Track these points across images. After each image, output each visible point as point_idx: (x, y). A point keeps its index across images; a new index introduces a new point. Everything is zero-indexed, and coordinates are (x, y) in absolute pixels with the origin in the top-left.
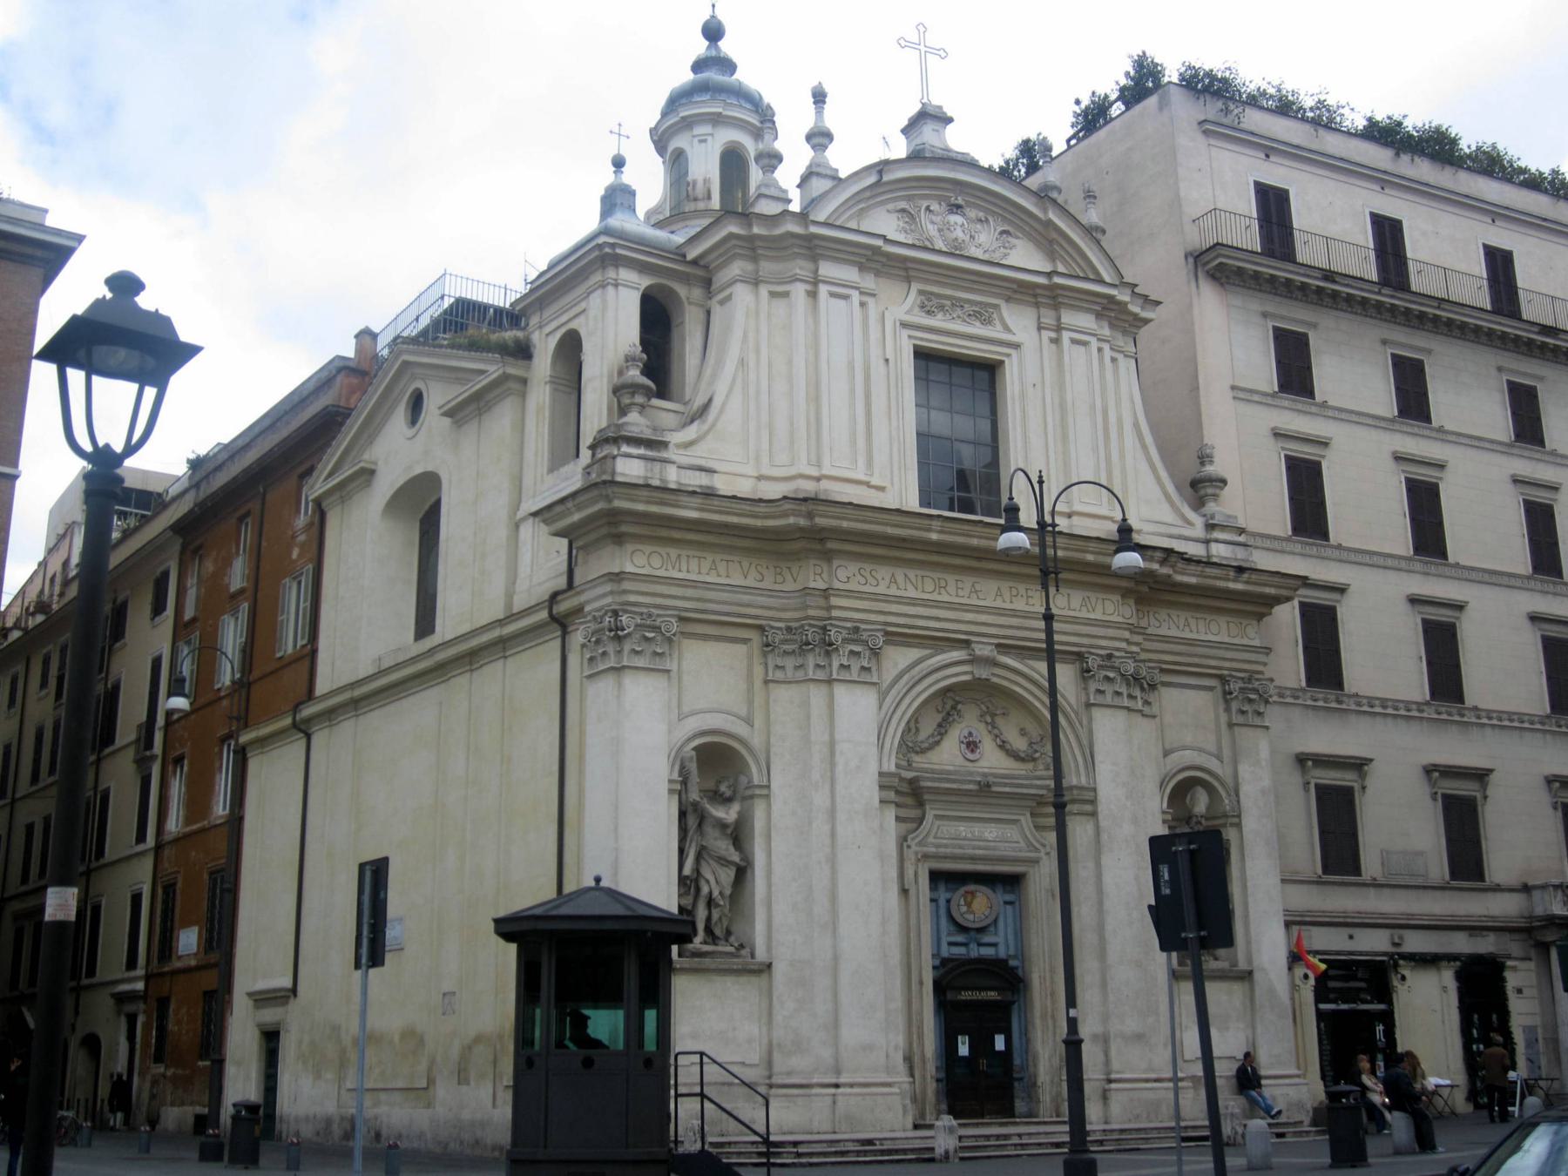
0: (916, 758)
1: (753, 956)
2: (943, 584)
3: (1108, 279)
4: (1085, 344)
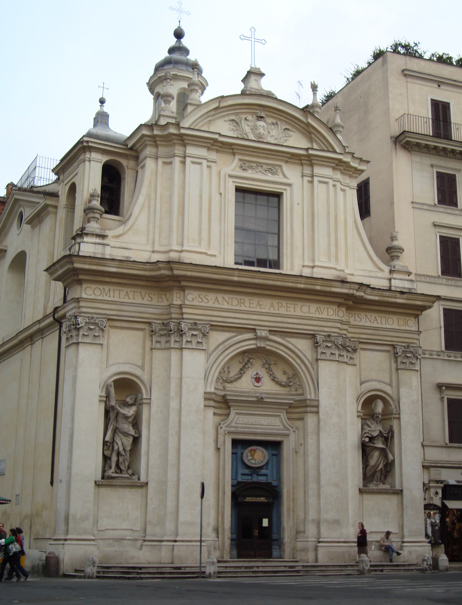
0: (227, 385)
1: (139, 479)
2: (242, 301)
3: (338, 151)
4: (326, 183)
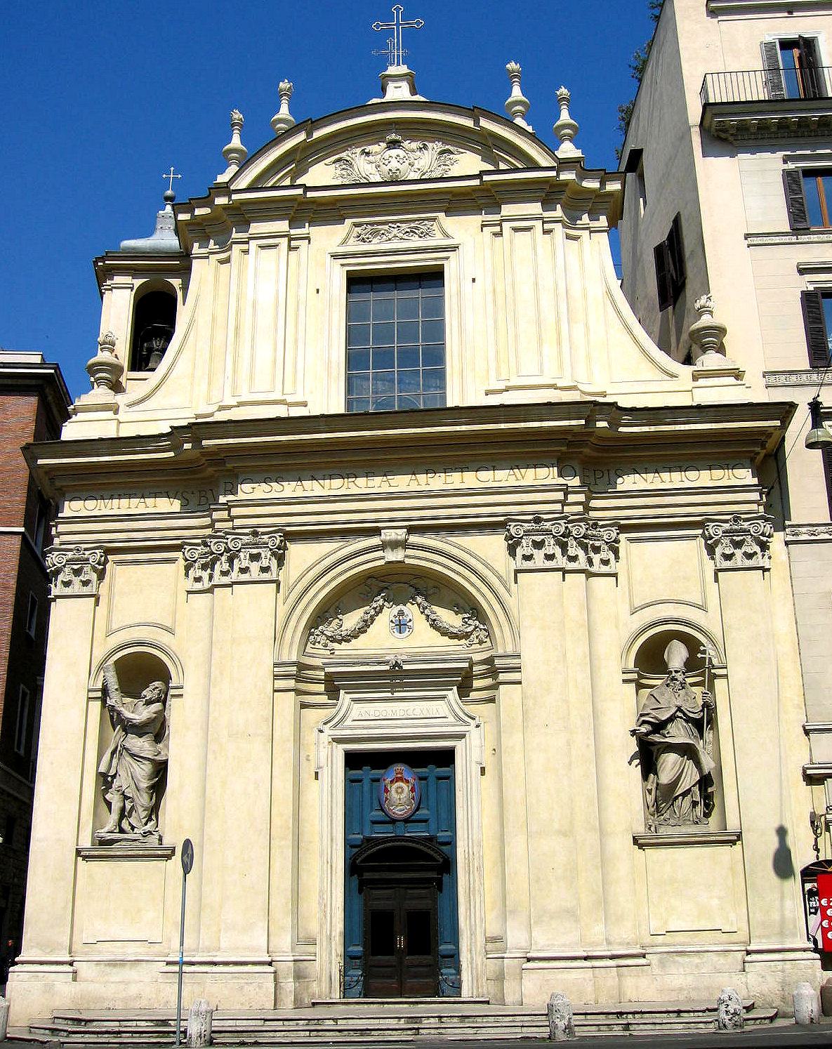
0: (336, 645)
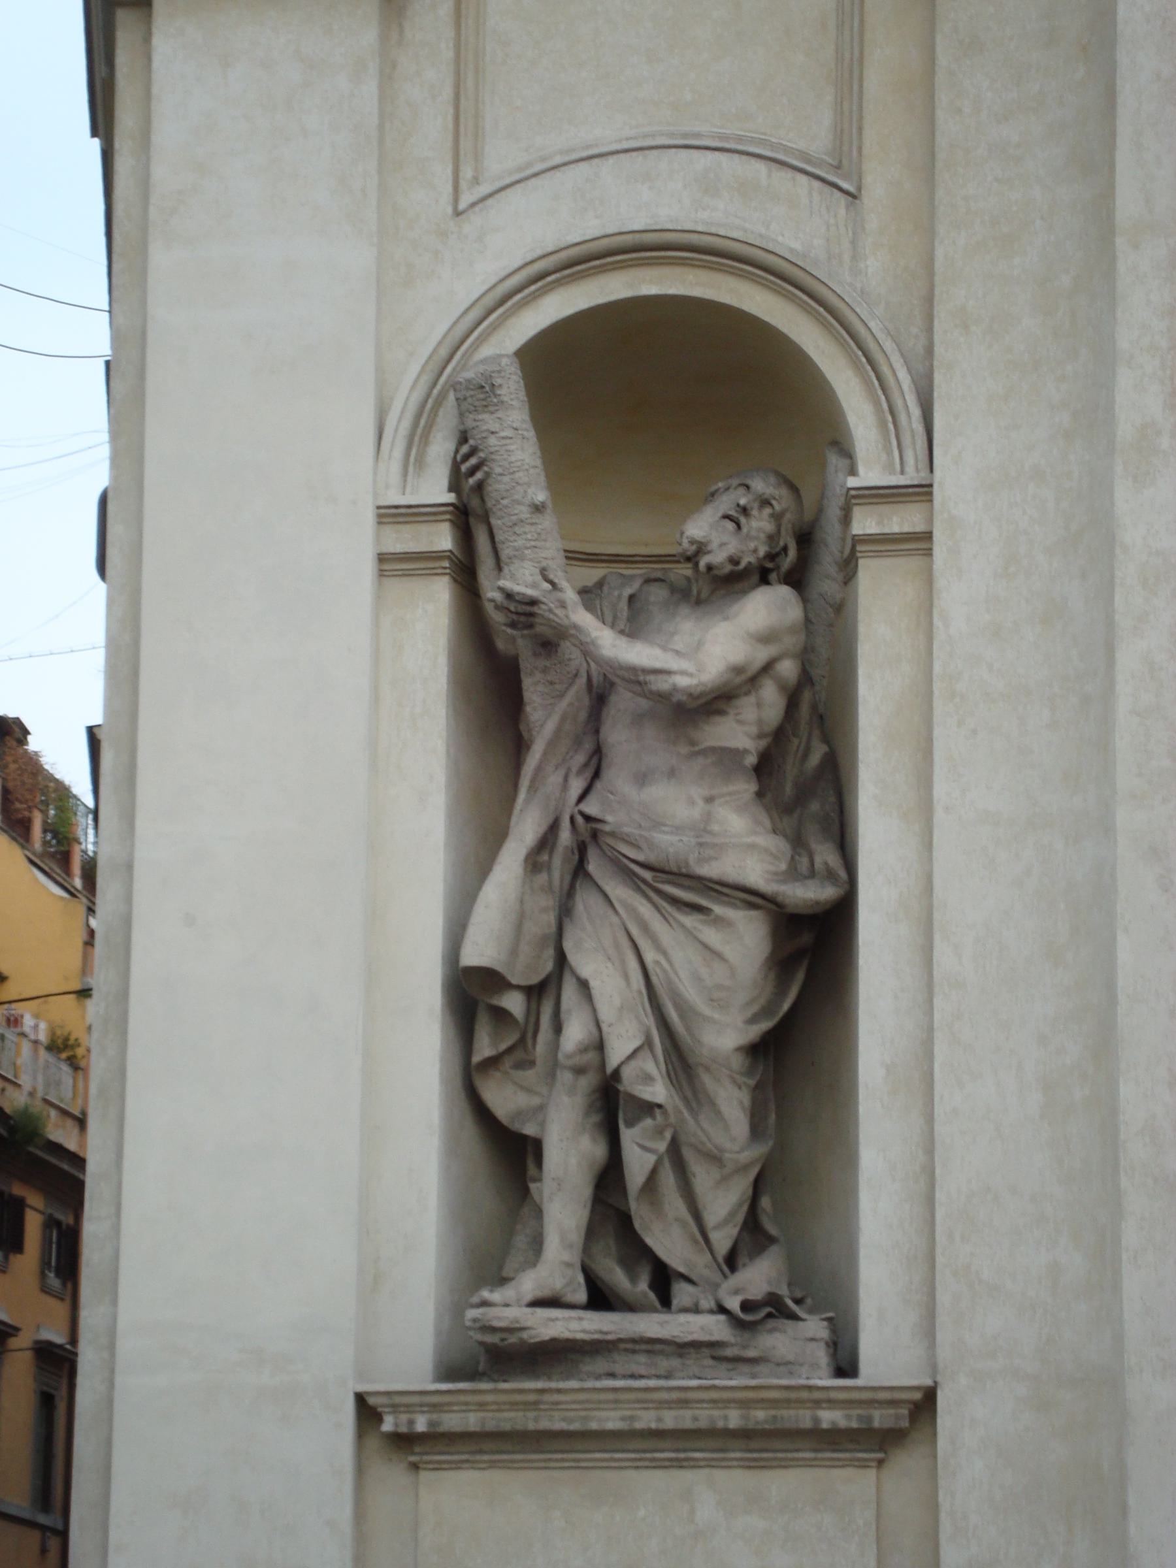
1: (846, 1367)
